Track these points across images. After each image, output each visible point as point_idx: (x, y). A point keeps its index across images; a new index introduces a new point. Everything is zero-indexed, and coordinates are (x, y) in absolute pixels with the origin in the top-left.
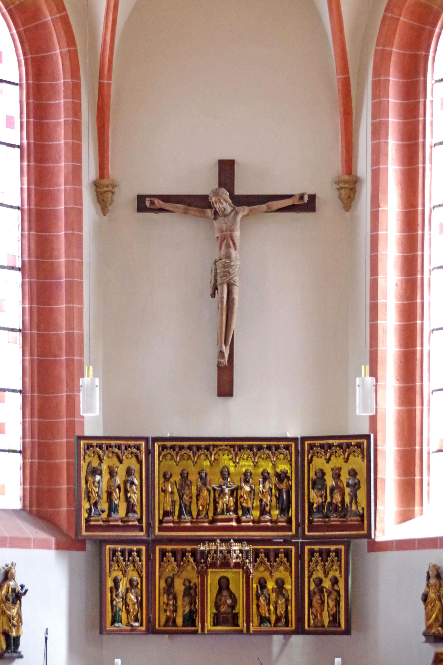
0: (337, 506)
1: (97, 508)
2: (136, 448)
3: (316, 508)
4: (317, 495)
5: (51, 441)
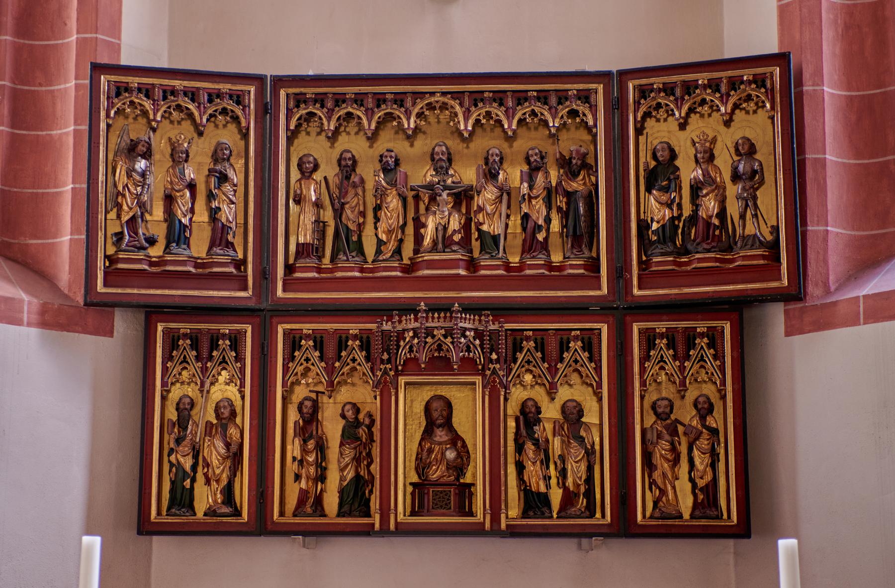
0: (708, 224)
1: (136, 233)
2: (235, 98)
3: (655, 232)
4: (660, 203)
5: (44, 89)
